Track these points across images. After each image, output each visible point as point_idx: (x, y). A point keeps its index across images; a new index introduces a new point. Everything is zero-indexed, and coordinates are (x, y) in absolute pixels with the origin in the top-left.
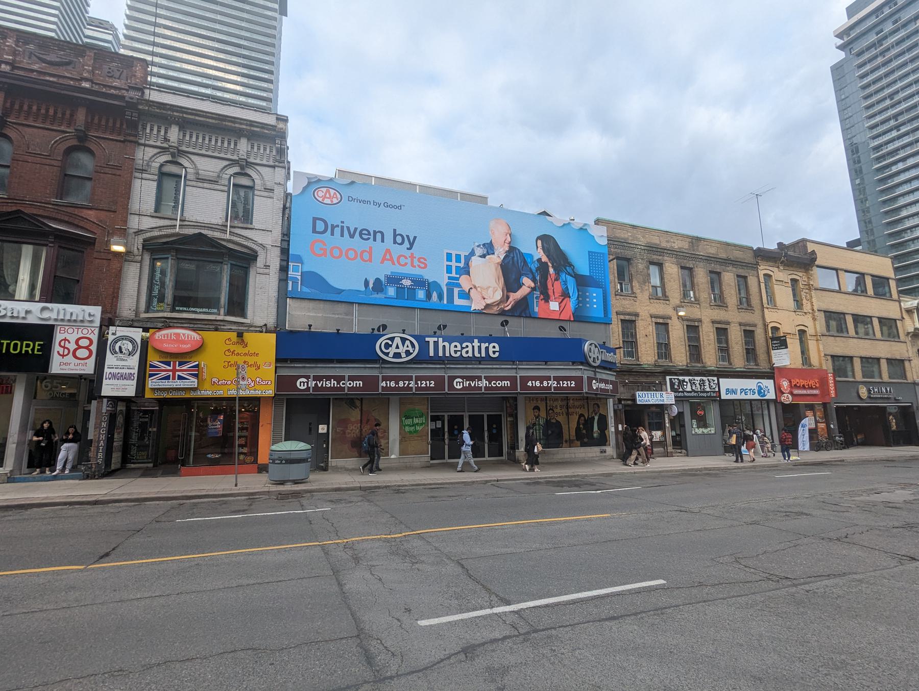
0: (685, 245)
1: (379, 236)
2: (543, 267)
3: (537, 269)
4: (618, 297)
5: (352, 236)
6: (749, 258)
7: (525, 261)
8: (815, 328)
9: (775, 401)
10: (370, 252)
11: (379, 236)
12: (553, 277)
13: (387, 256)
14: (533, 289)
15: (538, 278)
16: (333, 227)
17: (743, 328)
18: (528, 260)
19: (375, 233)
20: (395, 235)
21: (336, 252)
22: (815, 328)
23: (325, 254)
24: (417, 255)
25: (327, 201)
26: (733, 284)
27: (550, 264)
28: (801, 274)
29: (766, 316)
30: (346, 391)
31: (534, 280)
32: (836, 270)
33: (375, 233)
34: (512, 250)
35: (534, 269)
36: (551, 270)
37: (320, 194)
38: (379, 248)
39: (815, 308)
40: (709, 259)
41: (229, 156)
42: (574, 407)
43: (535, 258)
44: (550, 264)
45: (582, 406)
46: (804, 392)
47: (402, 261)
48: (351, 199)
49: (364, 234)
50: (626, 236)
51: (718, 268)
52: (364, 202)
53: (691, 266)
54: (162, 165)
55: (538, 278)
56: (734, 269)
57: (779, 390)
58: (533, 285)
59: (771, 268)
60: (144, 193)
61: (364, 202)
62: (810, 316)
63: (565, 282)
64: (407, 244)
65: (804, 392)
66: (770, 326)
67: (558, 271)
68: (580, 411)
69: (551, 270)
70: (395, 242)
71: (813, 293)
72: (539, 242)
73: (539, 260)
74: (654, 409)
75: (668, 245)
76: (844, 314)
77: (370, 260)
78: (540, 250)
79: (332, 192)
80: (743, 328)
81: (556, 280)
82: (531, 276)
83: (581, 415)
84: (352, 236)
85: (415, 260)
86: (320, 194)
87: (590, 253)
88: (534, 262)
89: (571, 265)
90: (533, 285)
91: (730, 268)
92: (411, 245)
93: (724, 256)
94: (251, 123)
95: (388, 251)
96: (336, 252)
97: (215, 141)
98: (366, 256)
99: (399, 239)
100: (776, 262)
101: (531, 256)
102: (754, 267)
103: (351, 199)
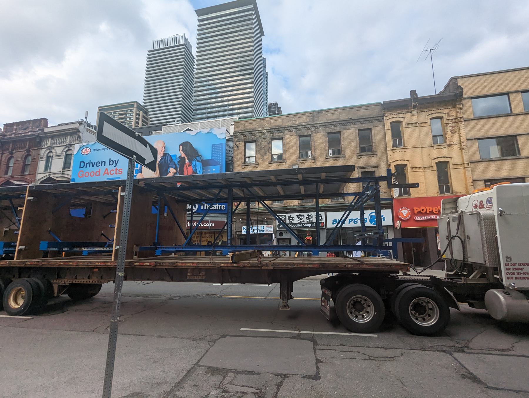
0: (306, 120)
1: (103, 163)
2: (182, 160)
3: (178, 162)
4: (243, 167)
5: (93, 166)
6: (375, 112)
7: (172, 159)
8: (463, 157)
9: (393, 227)
10: (99, 172)
11: (103, 163)
12: (188, 165)
13: (106, 172)
14: (175, 174)
15: (178, 167)
16: (87, 164)
17: (361, 170)
18: (174, 158)
19: (102, 162)
20: (110, 161)
21: (87, 175)
22: (463, 157)
23: (83, 176)
24: (118, 169)
25: (86, 153)
26: (354, 138)
27: (186, 158)
28: (446, 111)
29: (389, 157)
30: (210, 228)
31: (176, 168)
32: (507, 94)
33: (102, 162)
34: (165, 154)
35: (176, 162)
36: (187, 161)
37: (84, 151)
38: (102, 168)
39: (464, 138)
40: (328, 124)
41: (64, 144)
42: (205, 237)
43: (178, 157)
44: (186, 158)
45: (209, 237)
46: (426, 218)
47: (112, 172)
48: (94, 150)
49: (98, 164)
50: (254, 126)
51: (337, 129)
52: (99, 150)
53: (310, 133)
54: (48, 154)
55: (178, 167)
56: (357, 126)
57: (395, 217)
58: (175, 171)
59: (401, 115)
60: (42, 165)
61: (99, 150)
62: (456, 148)
63: (195, 166)
64: (114, 164)
65: (426, 218)
66: (393, 165)
67: (190, 160)
68: (209, 239)
69: (187, 161)
70: (110, 165)
71: (462, 125)
72: (181, 147)
73: (180, 157)
74: (266, 237)
75: (290, 124)
76: (515, 136)
77: (99, 175)
78: (181, 152)
79: (88, 149)
80: (361, 170)
81: (189, 166)
82: (174, 166)
83: (209, 242)
84: (93, 166)
85: (117, 171)
86: (84, 151)
87: (213, 146)
88: (177, 159)
89: (199, 155)
90: (175, 171)
91: (352, 126)
92: (116, 164)
93: (346, 118)
94: (69, 129)
95: (107, 169)
96: (87, 175)
97: (61, 140)
98: (98, 173)
99: (111, 163)
100: (408, 109)
101: (176, 156)
102: (380, 119)
103: (94, 150)
